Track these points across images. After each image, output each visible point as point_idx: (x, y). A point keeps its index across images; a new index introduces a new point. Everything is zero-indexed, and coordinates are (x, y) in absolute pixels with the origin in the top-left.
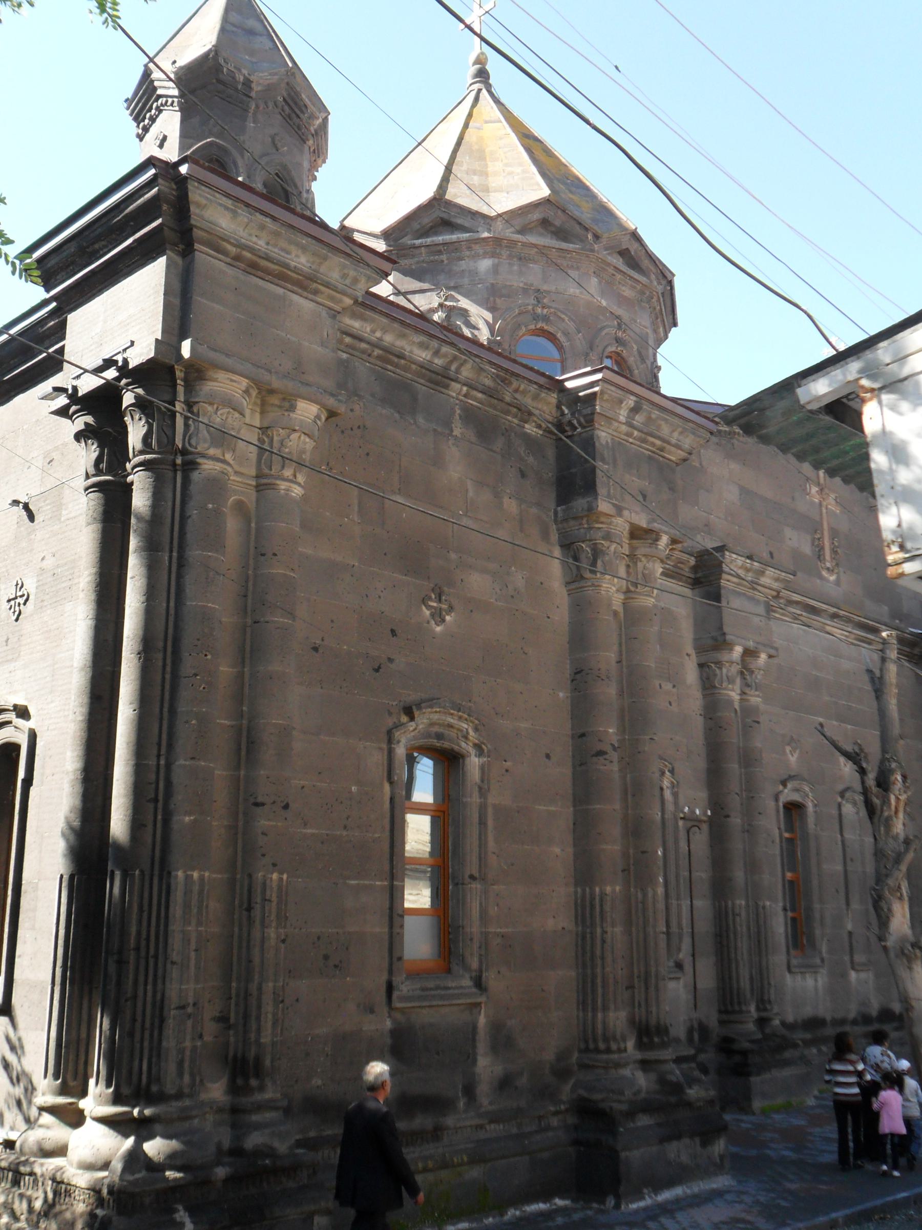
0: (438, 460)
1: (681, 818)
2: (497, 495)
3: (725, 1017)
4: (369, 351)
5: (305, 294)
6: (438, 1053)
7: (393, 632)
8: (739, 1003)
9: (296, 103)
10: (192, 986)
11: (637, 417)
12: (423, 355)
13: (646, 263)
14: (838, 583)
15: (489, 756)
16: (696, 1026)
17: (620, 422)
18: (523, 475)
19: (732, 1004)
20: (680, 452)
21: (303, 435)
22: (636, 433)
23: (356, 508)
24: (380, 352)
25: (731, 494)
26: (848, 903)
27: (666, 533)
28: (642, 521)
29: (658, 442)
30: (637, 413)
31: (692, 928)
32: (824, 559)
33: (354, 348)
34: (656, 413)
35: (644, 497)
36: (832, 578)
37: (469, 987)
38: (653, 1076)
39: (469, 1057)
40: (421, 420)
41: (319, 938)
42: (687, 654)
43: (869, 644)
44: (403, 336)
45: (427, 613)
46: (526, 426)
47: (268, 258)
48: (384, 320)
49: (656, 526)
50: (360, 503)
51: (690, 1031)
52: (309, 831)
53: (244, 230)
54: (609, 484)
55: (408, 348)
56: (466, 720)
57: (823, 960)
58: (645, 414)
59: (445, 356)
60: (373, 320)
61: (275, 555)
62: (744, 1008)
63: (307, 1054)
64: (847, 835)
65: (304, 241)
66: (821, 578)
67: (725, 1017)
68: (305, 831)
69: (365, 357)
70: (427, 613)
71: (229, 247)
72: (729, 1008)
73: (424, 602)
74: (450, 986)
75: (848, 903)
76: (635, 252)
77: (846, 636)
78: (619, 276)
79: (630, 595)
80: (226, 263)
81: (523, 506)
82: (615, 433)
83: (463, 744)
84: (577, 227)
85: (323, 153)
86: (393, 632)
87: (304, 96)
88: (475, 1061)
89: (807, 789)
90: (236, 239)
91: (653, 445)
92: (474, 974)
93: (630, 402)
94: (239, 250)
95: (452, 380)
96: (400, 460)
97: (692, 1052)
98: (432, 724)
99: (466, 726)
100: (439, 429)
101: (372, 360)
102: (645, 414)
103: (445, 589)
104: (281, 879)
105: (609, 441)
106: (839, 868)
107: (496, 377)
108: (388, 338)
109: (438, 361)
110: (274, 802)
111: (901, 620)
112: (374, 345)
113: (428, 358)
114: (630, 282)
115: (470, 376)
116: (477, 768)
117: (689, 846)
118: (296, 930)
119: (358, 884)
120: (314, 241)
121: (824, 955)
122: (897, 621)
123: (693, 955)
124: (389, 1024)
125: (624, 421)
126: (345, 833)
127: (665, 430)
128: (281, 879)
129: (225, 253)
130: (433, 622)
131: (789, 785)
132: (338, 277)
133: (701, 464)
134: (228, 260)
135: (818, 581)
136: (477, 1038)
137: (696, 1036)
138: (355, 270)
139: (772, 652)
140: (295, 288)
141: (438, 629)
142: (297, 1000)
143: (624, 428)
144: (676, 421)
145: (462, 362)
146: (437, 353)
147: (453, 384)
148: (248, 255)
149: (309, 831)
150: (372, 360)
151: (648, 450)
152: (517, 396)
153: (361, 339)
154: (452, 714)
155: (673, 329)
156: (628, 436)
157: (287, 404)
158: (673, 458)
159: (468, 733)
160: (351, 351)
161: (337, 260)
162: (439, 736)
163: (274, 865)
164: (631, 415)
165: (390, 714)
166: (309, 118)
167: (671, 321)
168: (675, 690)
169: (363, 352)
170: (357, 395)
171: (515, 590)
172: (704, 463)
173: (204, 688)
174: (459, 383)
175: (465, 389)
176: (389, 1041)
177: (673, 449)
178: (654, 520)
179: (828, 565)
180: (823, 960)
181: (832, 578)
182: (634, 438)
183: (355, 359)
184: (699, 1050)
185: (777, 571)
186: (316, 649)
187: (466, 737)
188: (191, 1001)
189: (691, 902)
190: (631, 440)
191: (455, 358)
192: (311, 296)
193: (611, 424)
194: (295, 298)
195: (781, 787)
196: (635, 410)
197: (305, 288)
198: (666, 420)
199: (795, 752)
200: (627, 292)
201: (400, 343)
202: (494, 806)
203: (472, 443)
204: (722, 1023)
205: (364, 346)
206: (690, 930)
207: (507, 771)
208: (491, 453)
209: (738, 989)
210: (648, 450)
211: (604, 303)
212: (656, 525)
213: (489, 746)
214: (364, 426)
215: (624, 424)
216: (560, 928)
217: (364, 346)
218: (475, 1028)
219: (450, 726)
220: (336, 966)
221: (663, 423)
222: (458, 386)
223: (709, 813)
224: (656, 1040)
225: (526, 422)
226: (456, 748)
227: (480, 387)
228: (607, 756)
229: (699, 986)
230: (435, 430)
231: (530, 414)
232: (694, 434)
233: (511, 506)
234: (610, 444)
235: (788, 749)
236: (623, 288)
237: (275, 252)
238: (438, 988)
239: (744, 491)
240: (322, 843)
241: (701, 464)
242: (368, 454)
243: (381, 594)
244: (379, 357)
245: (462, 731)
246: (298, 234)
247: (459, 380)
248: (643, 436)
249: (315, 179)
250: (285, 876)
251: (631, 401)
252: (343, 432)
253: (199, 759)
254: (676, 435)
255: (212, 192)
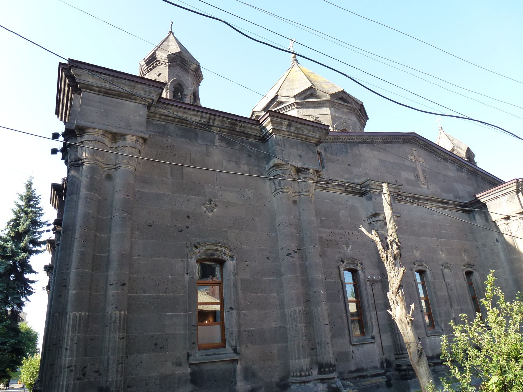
0: (208, 154)
1: (368, 281)
2: (237, 164)
3: (397, 356)
4: (173, 120)
5: (131, 100)
6: (215, 381)
7: (188, 217)
8: (402, 350)
9: (184, 62)
10: (75, 358)
11: (291, 128)
12: (196, 119)
13: (350, 100)
14: (428, 188)
15: (236, 260)
16: (384, 361)
17: (284, 131)
18: (249, 156)
19: (399, 351)
20: (315, 139)
21: (130, 147)
22: (293, 134)
23: (170, 174)
24: (178, 120)
25: (376, 162)
26: (451, 306)
27: (311, 168)
28: (299, 165)
29: (304, 137)
30: (291, 127)
31: (378, 322)
32: (420, 180)
33: (167, 120)
34: (299, 126)
35: (301, 157)
36: (425, 187)
37: (231, 353)
38: (326, 385)
39: (232, 382)
40: (200, 141)
41: (152, 337)
42: (363, 220)
43: (446, 209)
44: (185, 113)
45: (205, 209)
46: (250, 139)
47: (110, 90)
48: (176, 108)
49: (306, 166)
50: (171, 172)
51: (382, 363)
52: (147, 295)
53: (99, 81)
54: (282, 153)
55: (189, 117)
56: (224, 247)
57: (443, 330)
58: (294, 126)
59: (205, 118)
60: (171, 109)
61: (120, 191)
62: (404, 352)
63: (147, 384)
64: (447, 280)
65: (124, 81)
66: (420, 187)
67: (397, 356)
68: (145, 295)
69: (172, 122)
70: (205, 209)
71: (95, 88)
72: (398, 353)
73: (204, 205)
74: (221, 353)
75: (451, 306)
76: (345, 97)
77: (435, 207)
78: (341, 106)
79: (300, 194)
80: (95, 94)
81: (250, 167)
82: (283, 135)
83: (224, 257)
84: (323, 93)
85: (201, 77)
86: (188, 217)
87: (186, 59)
88: (235, 384)
89: (425, 265)
90: (97, 85)
91: (302, 138)
92: (233, 348)
93: (286, 122)
94: (99, 89)
95: (212, 126)
96: (190, 156)
97: (383, 371)
98: (208, 250)
99: (224, 249)
100: (209, 144)
101: (176, 123)
102: (294, 126)
103: (213, 199)
104: (120, 314)
105: (281, 139)
106: (446, 293)
107: (230, 123)
108: (180, 114)
109: (204, 120)
110: (117, 283)
111: (459, 199)
112: (175, 118)
113: (199, 119)
114: (345, 107)
115: (219, 124)
116: (232, 265)
117: (373, 291)
118: (141, 334)
119: (172, 314)
120: (128, 81)
121: (443, 328)
122: (458, 199)
123: (380, 333)
124: (189, 370)
125: (286, 130)
126: (165, 294)
127: (306, 132)
128: (125, 314)
129: (94, 90)
130: (208, 212)
131: (417, 264)
132: (143, 92)
133: (360, 153)
134: (96, 93)
135: (419, 188)
136: (237, 374)
137: (385, 365)
138: (148, 89)
139: (398, 215)
140: (126, 99)
141: (210, 214)
142: (141, 362)
143: (286, 133)
144: (309, 127)
145: (214, 119)
146: (202, 117)
147: (213, 128)
148: (104, 90)
149: (147, 295)
150: (176, 123)
151: (300, 140)
152: (241, 128)
153: (168, 116)
154: (216, 245)
155: (368, 120)
156: (289, 136)
157: (122, 138)
158: (314, 142)
159: (225, 252)
160: (166, 121)
161: (139, 86)
162: (212, 254)
163: (116, 308)
164: (288, 128)
165: (187, 247)
166: (189, 65)
167: (366, 118)
168: (359, 234)
169: (171, 120)
170: (170, 135)
171: (248, 197)
172: (362, 153)
173: (84, 242)
174: (215, 127)
175: (218, 129)
176: (189, 377)
177: (312, 138)
178: (304, 164)
179: (423, 182)
180: (443, 330)
181: (425, 187)
182: (293, 136)
183: (168, 123)
184: (387, 371)
185: (394, 185)
186: (150, 226)
187: (225, 254)
188: (73, 364)
189: (376, 312)
190: (291, 137)
191: (210, 119)
192: (133, 101)
193: (280, 132)
194: (127, 102)
195: (413, 265)
196: (289, 125)
197: (130, 98)
198: (305, 128)
199: (418, 251)
200: (345, 110)
201: (185, 116)
202: (241, 280)
203: (225, 147)
204: (396, 359)
205: (170, 118)
206: (377, 323)
207: (247, 265)
208: (234, 150)
209: (400, 344)
210: (300, 140)
211: (337, 115)
212: (306, 166)
213: (237, 256)
214: (173, 146)
215: (286, 131)
216: (278, 326)
217: (170, 118)
218: (235, 370)
219: (217, 250)
220: (161, 348)
221: (303, 129)
222: (215, 128)
223: (380, 278)
224: (327, 369)
225: (249, 138)
226: (221, 258)
227: (225, 127)
228: (291, 255)
229: (383, 345)
230: (207, 144)
231: (250, 135)
232: (319, 131)
233: (245, 168)
234: (282, 140)
235: (414, 251)
236: (344, 109)
237: (114, 87)
238: (214, 354)
239: (381, 161)
240: (154, 299)
241: (360, 153)
242: (175, 155)
243: (182, 203)
244: (178, 122)
245: (222, 251)
246: (121, 80)
247: (215, 126)
248: (296, 135)
249: (200, 85)
250: (126, 312)
251: (286, 122)
252: (163, 148)
253: (79, 269)
254: (311, 133)
255: (82, 70)
